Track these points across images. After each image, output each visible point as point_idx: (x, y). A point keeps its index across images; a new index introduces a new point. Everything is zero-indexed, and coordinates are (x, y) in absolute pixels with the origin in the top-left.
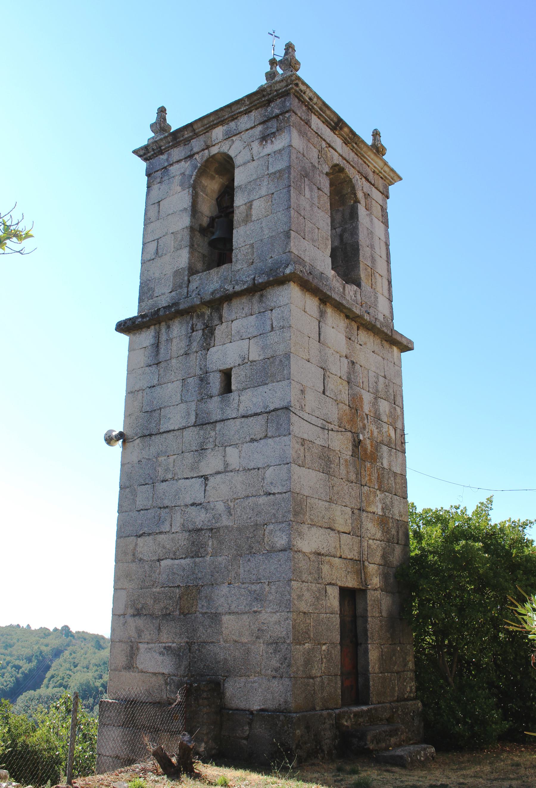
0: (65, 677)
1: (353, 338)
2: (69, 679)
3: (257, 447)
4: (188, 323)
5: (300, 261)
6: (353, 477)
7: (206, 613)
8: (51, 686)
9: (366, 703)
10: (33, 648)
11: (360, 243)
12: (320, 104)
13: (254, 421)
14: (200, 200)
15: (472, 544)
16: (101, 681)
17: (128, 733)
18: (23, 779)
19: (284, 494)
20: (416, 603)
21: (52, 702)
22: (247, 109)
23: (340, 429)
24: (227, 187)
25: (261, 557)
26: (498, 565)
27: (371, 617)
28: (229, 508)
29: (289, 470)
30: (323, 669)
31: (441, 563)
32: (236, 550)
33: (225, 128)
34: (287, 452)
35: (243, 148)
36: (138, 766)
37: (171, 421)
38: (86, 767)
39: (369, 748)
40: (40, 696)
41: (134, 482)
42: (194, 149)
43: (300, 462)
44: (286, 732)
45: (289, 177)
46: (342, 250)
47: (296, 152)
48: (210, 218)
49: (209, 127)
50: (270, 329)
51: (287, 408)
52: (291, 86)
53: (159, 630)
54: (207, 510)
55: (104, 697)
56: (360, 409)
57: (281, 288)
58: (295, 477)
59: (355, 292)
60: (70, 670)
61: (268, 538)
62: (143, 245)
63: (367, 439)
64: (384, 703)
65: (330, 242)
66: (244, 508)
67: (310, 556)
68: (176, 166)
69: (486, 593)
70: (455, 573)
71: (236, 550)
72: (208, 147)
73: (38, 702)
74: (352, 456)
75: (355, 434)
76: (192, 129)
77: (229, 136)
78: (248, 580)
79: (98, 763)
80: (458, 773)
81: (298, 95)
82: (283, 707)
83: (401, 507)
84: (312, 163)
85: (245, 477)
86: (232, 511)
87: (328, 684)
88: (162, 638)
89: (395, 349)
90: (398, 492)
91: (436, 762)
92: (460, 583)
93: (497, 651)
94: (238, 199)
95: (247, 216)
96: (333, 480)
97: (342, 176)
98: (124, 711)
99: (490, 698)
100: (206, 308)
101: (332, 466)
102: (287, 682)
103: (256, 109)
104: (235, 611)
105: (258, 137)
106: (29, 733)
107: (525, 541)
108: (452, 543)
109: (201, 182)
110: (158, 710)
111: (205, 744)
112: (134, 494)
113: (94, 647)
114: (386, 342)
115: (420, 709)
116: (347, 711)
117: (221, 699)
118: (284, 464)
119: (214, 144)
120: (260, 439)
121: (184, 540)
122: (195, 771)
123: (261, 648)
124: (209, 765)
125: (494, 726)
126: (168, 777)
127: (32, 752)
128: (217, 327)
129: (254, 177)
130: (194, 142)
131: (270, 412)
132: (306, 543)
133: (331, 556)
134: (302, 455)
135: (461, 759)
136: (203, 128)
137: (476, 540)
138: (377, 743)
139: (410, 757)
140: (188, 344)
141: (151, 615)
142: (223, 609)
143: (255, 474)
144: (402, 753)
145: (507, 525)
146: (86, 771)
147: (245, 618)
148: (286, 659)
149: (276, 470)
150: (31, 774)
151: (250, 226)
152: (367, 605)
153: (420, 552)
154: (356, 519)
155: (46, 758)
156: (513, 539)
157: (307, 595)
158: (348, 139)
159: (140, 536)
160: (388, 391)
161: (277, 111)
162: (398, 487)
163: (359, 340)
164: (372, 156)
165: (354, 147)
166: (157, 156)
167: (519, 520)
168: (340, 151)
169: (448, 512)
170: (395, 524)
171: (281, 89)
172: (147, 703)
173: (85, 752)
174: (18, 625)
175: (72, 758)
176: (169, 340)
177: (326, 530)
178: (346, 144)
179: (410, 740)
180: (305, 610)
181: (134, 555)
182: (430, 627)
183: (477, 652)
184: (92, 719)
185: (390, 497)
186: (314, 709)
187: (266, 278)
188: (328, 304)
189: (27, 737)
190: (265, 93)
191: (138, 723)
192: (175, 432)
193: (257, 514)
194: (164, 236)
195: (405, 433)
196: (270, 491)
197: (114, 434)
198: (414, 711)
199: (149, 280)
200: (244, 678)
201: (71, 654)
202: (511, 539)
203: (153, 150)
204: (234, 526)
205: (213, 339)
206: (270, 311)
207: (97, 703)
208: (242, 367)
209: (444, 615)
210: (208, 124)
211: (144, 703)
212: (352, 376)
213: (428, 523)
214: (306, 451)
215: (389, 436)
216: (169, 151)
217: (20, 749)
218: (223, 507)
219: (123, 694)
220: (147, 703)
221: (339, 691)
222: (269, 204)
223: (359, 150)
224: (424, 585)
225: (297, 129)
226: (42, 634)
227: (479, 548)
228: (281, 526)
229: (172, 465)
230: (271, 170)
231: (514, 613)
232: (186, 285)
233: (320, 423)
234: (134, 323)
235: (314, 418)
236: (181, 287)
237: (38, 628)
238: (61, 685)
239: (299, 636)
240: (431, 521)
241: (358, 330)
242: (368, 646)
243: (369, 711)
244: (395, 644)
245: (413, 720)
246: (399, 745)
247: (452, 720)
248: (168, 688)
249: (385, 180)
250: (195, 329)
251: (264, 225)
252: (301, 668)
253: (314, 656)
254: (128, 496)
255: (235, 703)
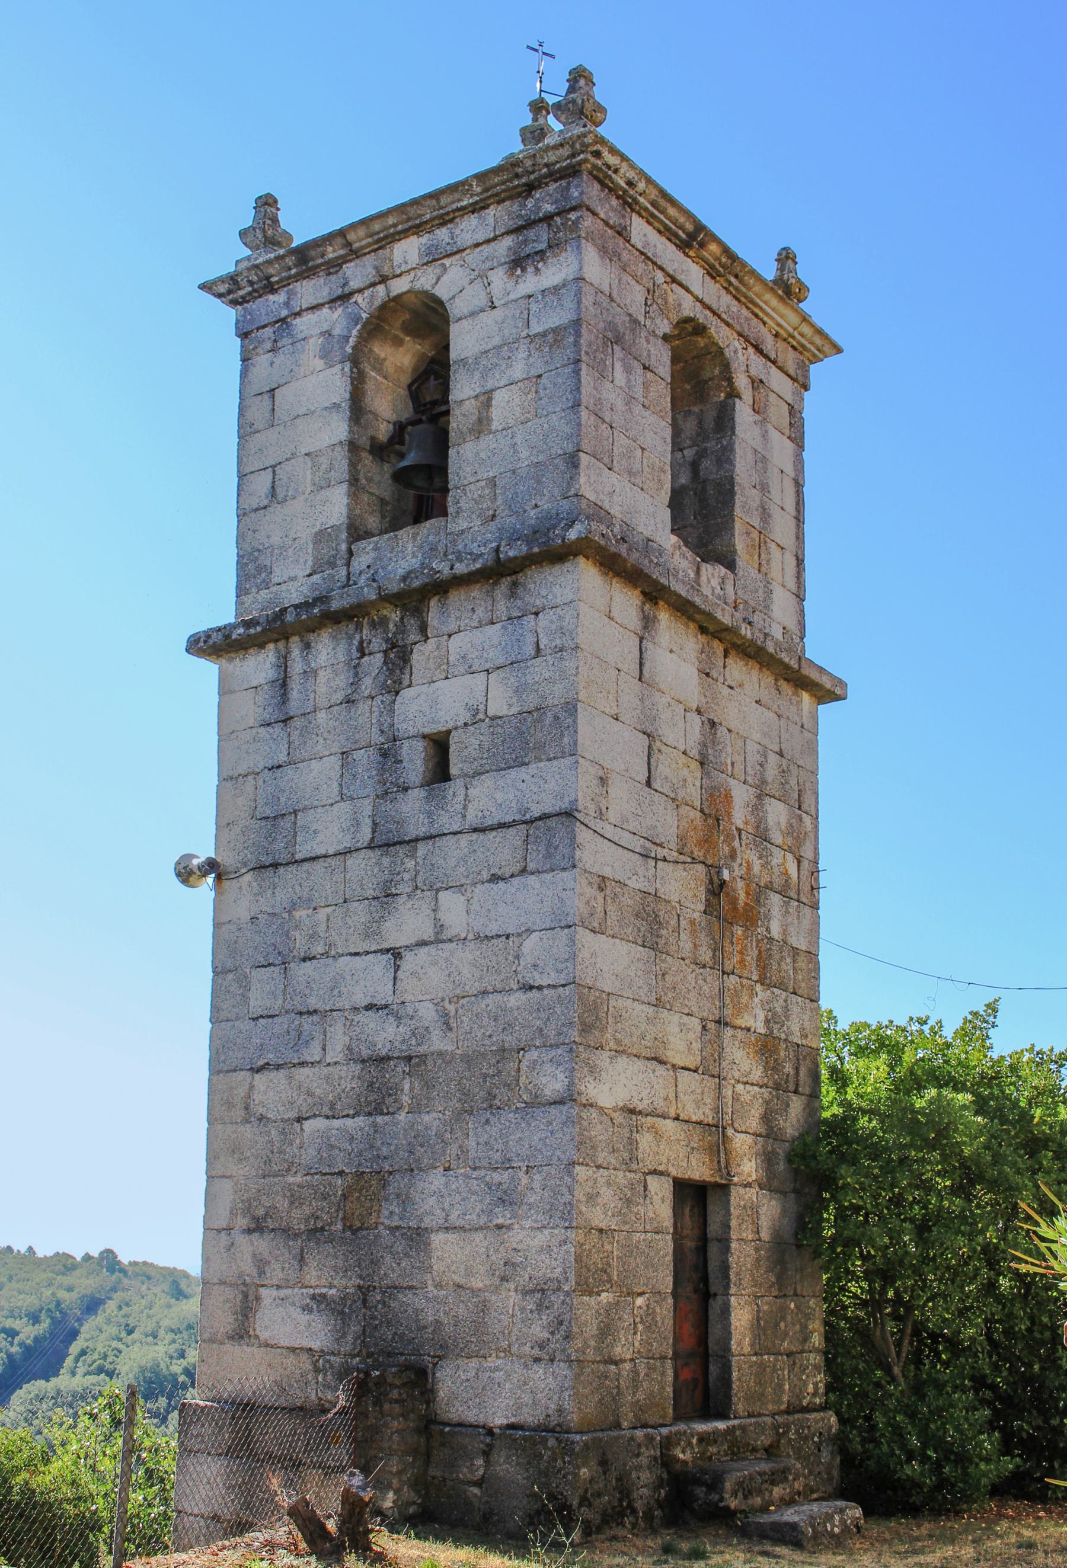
0: (109, 1353)
1: (714, 673)
2: (117, 1357)
3: (505, 893)
4: (351, 638)
5: (599, 514)
6: (706, 955)
7: (398, 1228)
8: (80, 1371)
9: (723, 1416)
10: (41, 1294)
11: (737, 479)
12: (653, 194)
13: (498, 840)
14: (369, 386)
15: (950, 1096)
16: (183, 1363)
17: (237, 1470)
18: (23, 1560)
19: (561, 989)
20: (829, 1214)
21: (83, 1404)
22: (476, 203)
23: (682, 858)
24: (433, 361)
25: (512, 1115)
26: (1003, 1140)
27: (738, 1240)
28: (447, 1014)
29: (572, 941)
30: (637, 1344)
31: (884, 1132)
32: (460, 1100)
33: (425, 239)
34: (568, 903)
35: (467, 280)
36: (258, 1537)
37: (320, 837)
38: (151, 1537)
39: (727, 1508)
40: (59, 1392)
41: (243, 960)
42: (351, 283)
43: (596, 924)
44: (559, 1471)
45: (576, 344)
46: (695, 494)
47: (593, 291)
48: (394, 424)
49: (386, 237)
50: (533, 653)
51: (568, 814)
52: (582, 156)
53: (302, 1260)
54: (400, 1018)
55: (188, 1395)
56: (726, 818)
57: (557, 569)
58: (584, 954)
59: (723, 580)
60: (120, 1340)
61: (527, 1077)
62: (239, 477)
63: (739, 880)
64: (760, 1415)
65: (670, 477)
66: (477, 1015)
67: (614, 1115)
68: (309, 318)
69: (975, 1197)
70: (913, 1153)
71: (460, 1100)
72: (384, 280)
73: (54, 1404)
74: (705, 912)
75: (713, 869)
76: (344, 241)
77: (434, 258)
78: (485, 1163)
79: (176, 1530)
80: (910, 1559)
81: (601, 176)
82: (554, 1421)
83: (806, 1017)
84: (630, 315)
85: (478, 953)
86: (451, 1021)
87: (647, 1375)
88: (308, 1277)
89: (805, 696)
90: (800, 988)
91: (864, 1537)
92: (923, 1174)
93: (993, 1315)
94: (459, 386)
95: (480, 420)
96: (664, 961)
97: (701, 342)
98: (230, 1424)
99: (977, 1410)
100: (391, 607)
101: (664, 932)
102: (562, 1369)
103: (498, 203)
104: (458, 1224)
105: (503, 260)
106: (36, 1466)
107: (1062, 1091)
108: (908, 1092)
109: (371, 351)
110: (300, 1424)
111: (395, 1493)
112: (245, 984)
113: (167, 1293)
114: (785, 683)
115: (834, 1430)
116: (685, 1432)
117: (428, 1403)
118: (561, 927)
119: (398, 272)
120: (512, 876)
121: (352, 1079)
122: (374, 1547)
123: (512, 1300)
124: (402, 1537)
125: (983, 1466)
126: (318, 1559)
127: (42, 1506)
128: (416, 648)
129: (496, 341)
130: (349, 269)
131: (532, 822)
132: (606, 1088)
133: (658, 1116)
134: (600, 909)
135: (916, 1533)
136: (370, 240)
137: (958, 1086)
138: (745, 1497)
139: (813, 1526)
140: (351, 680)
141: (284, 1230)
142: (432, 1220)
143: (500, 946)
144: (796, 1519)
145: (1025, 1059)
146: (151, 1545)
147: (478, 1240)
148: (561, 1323)
149: (545, 940)
150: (41, 1549)
151: (487, 442)
152: (730, 1215)
153: (841, 1110)
154: (710, 1040)
155: (70, 1517)
156: (1036, 1088)
157: (607, 1195)
158: (718, 266)
159: (259, 1070)
160: (787, 783)
161: (548, 208)
162: (800, 977)
163: (727, 676)
164: (774, 302)
165: (730, 283)
166: (260, 296)
167: (1051, 1050)
168: (699, 293)
169: (904, 1030)
170: (792, 1053)
171: (557, 162)
172: (276, 1409)
173: (150, 1505)
174: (9, 1249)
175: (124, 1519)
176: (310, 673)
177: (649, 1064)
178: (713, 278)
179: (812, 1491)
180: (603, 1225)
181: (247, 1108)
182: (859, 1263)
183: (953, 1315)
184: (164, 1439)
185: (783, 997)
186: (618, 1426)
187: (524, 548)
188: (661, 603)
189: (31, 1475)
190: (521, 170)
191: (258, 1448)
192: (328, 860)
193: (504, 1029)
194: (287, 460)
195: (821, 867)
196: (531, 982)
197: (195, 862)
198: (821, 1433)
199: (259, 550)
200: (474, 1360)
201: (120, 1308)
202: (1032, 1087)
203: (251, 283)
204: (457, 1051)
205: (407, 671)
206: (533, 616)
207: (175, 1408)
208: (471, 728)
209: (886, 1240)
210: (382, 231)
211: (271, 1408)
212: (710, 751)
213: (861, 1052)
214: (609, 901)
215: (786, 873)
216: (291, 287)
217: (18, 1498)
218: (434, 1013)
219: (228, 1389)
220: (276, 1409)
221: (669, 1390)
222: (530, 397)
223: (744, 289)
224: (847, 1176)
225: (595, 245)
226: (59, 1267)
227: (964, 1106)
228: (553, 1053)
229: (323, 927)
230: (536, 328)
231: (1030, 1238)
232: (344, 561)
233: (638, 844)
234: (227, 637)
235: (626, 834)
236: (332, 564)
237: (52, 1254)
238: (100, 1370)
239: (588, 1278)
240: (867, 1048)
241: (725, 656)
242: (729, 1300)
243: (730, 1431)
244: (785, 1296)
245: (819, 1450)
246: (789, 1502)
247: (898, 1452)
248: (320, 1379)
249: (801, 353)
250: (367, 652)
251: (518, 439)
252: (592, 1343)
253: (619, 1318)
254: (232, 989)
255: (457, 1410)
